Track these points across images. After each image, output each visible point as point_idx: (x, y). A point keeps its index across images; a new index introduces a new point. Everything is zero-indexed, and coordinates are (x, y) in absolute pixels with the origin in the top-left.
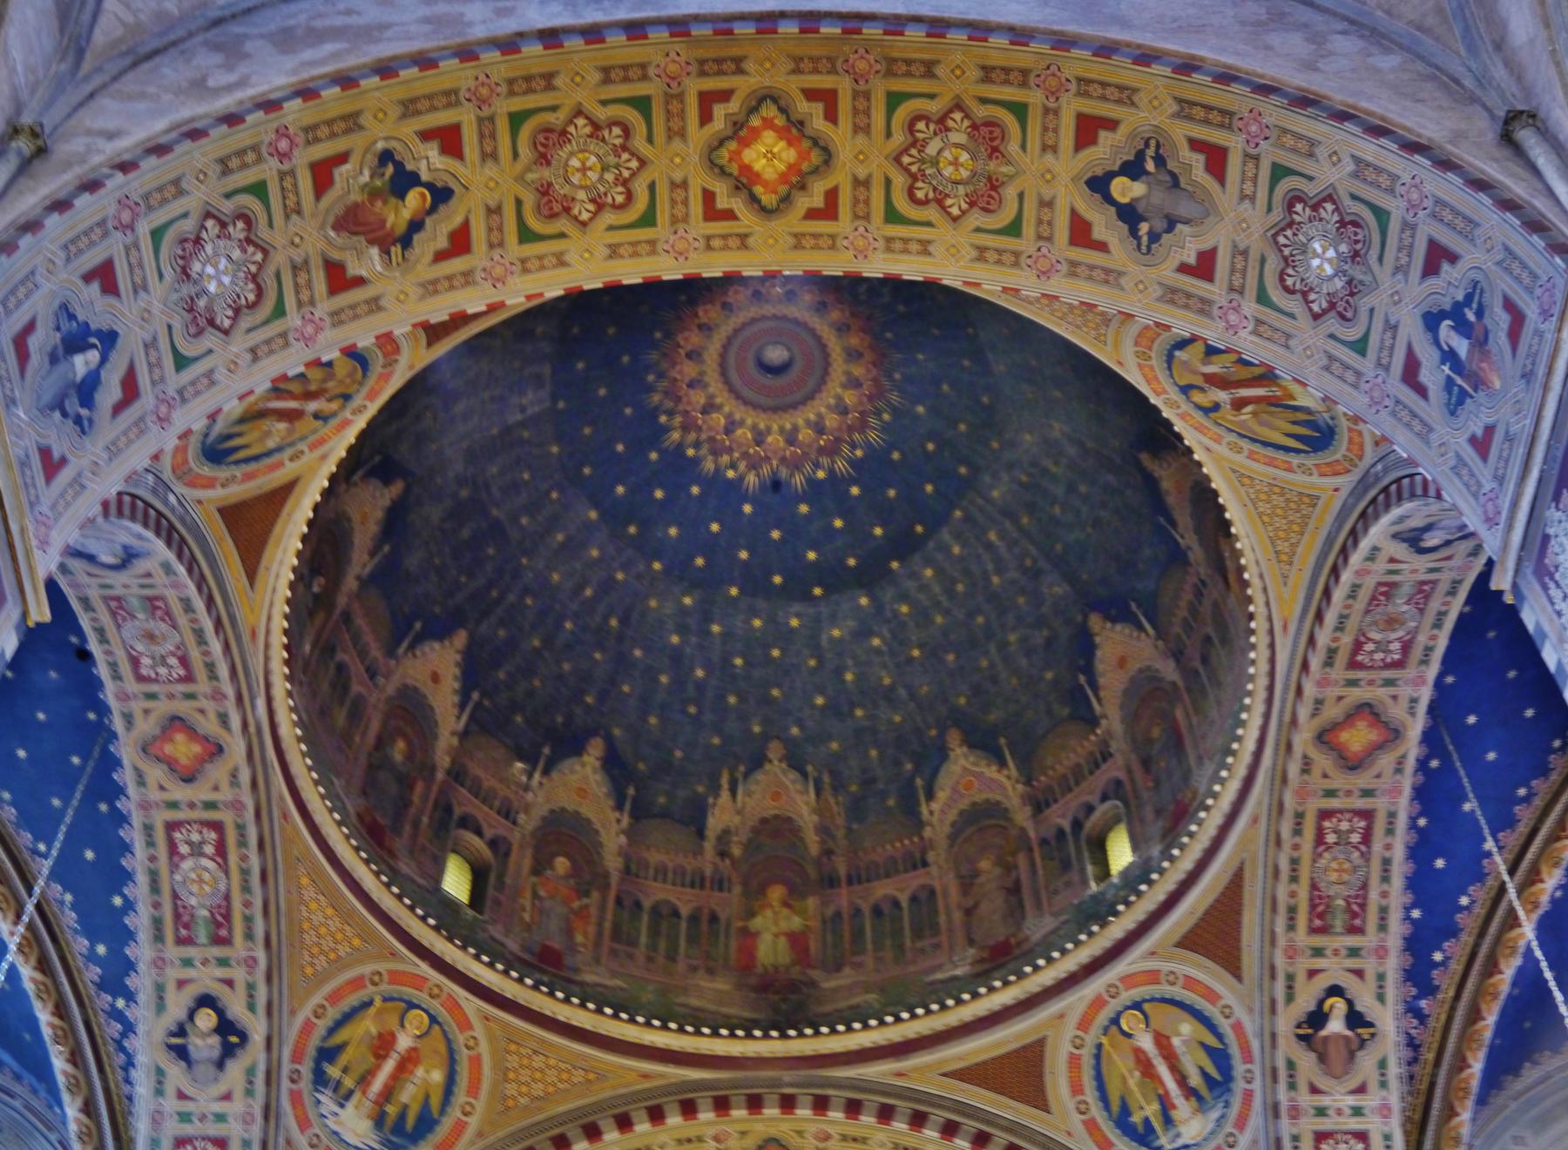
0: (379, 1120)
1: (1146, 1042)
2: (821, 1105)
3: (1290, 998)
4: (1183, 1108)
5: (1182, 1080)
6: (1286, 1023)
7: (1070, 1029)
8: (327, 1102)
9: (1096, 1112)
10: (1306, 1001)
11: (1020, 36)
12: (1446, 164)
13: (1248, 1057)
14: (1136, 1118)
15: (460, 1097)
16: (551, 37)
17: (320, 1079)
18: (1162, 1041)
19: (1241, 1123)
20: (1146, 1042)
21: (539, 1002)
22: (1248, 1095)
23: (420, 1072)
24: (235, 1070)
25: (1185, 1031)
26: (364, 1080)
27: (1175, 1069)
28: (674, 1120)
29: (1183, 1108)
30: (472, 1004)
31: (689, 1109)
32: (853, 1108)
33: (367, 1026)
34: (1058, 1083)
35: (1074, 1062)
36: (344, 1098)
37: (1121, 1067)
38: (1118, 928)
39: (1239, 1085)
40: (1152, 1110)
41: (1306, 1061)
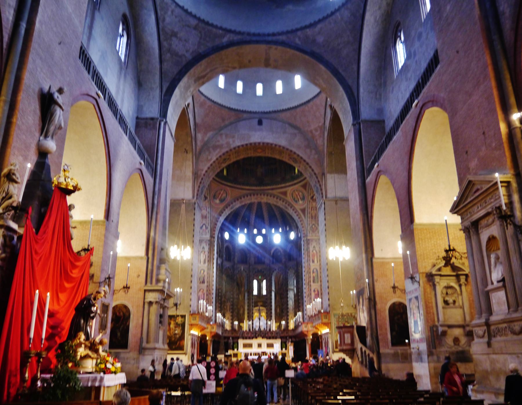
0: (220, 200)
1: (297, 193)
2: (264, 195)
3: (310, 195)
4: (300, 200)
5: (300, 198)
6: (310, 197)
7: (290, 190)
8: (215, 200)
9: (291, 198)
10: (312, 195)
11: (284, 148)
12: (317, 178)
13: (306, 197)
14: (296, 199)
15: (228, 196)
16: (239, 147)
17: (214, 198)
18: (299, 194)
19: (305, 203)
20: (297, 193)
21: (235, 186)
22: (306, 202)
23: (223, 195)
24: (207, 201)
25: (301, 194)
26: (218, 197)
27: (300, 196)
28: (249, 196)
29: (300, 200)
30: (228, 188)
31: (251, 195)
32: (267, 195)
33: (218, 192)
34: (288, 194)
35: (290, 194)
36: (216, 199)
37: (294, 195)
38: (295, 182)
39: (305, 200)
40: (297, 200)
41: (311, 201)
